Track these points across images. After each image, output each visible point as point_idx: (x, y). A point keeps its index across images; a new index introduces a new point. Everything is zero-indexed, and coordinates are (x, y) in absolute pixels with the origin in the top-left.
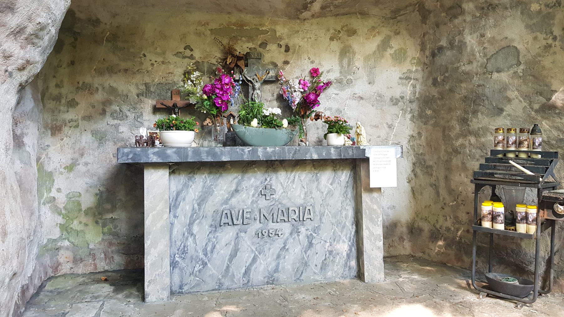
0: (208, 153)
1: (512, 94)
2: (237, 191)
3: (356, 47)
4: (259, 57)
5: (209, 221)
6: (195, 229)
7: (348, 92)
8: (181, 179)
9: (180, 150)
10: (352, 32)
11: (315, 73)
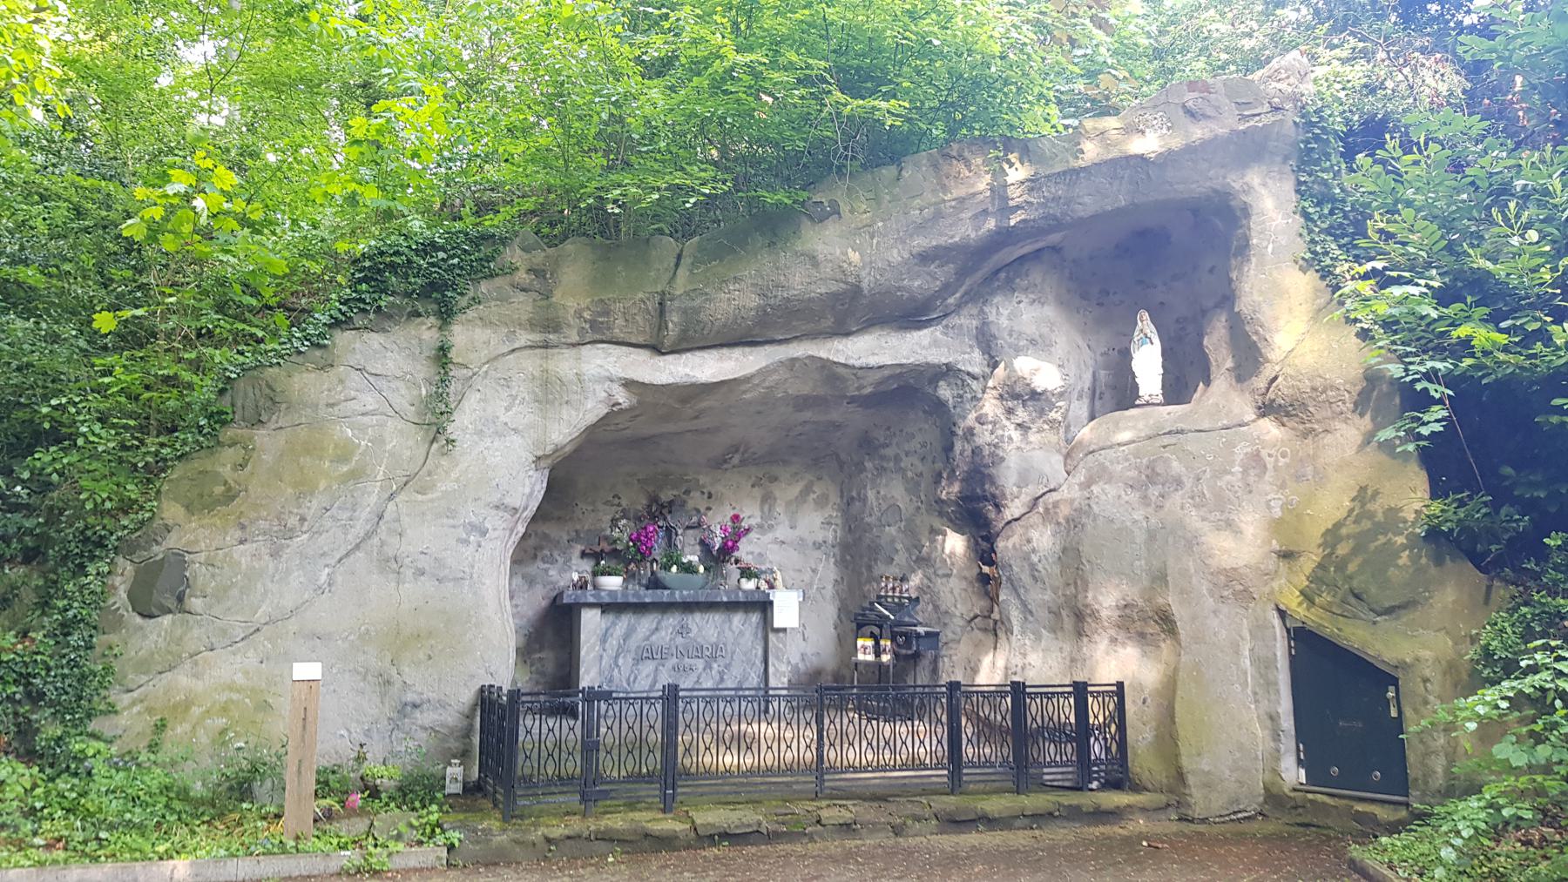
0: (634, 595)
1: (899, 546)
2: (657, 629)
3: (777, 493)
4: (683, 503)
5: (633, 655)
6: (621, 661)
7: (770, 536)
8: (611, 617)
9: (611, 593)
10: (774, 479)
11: (736, 518)
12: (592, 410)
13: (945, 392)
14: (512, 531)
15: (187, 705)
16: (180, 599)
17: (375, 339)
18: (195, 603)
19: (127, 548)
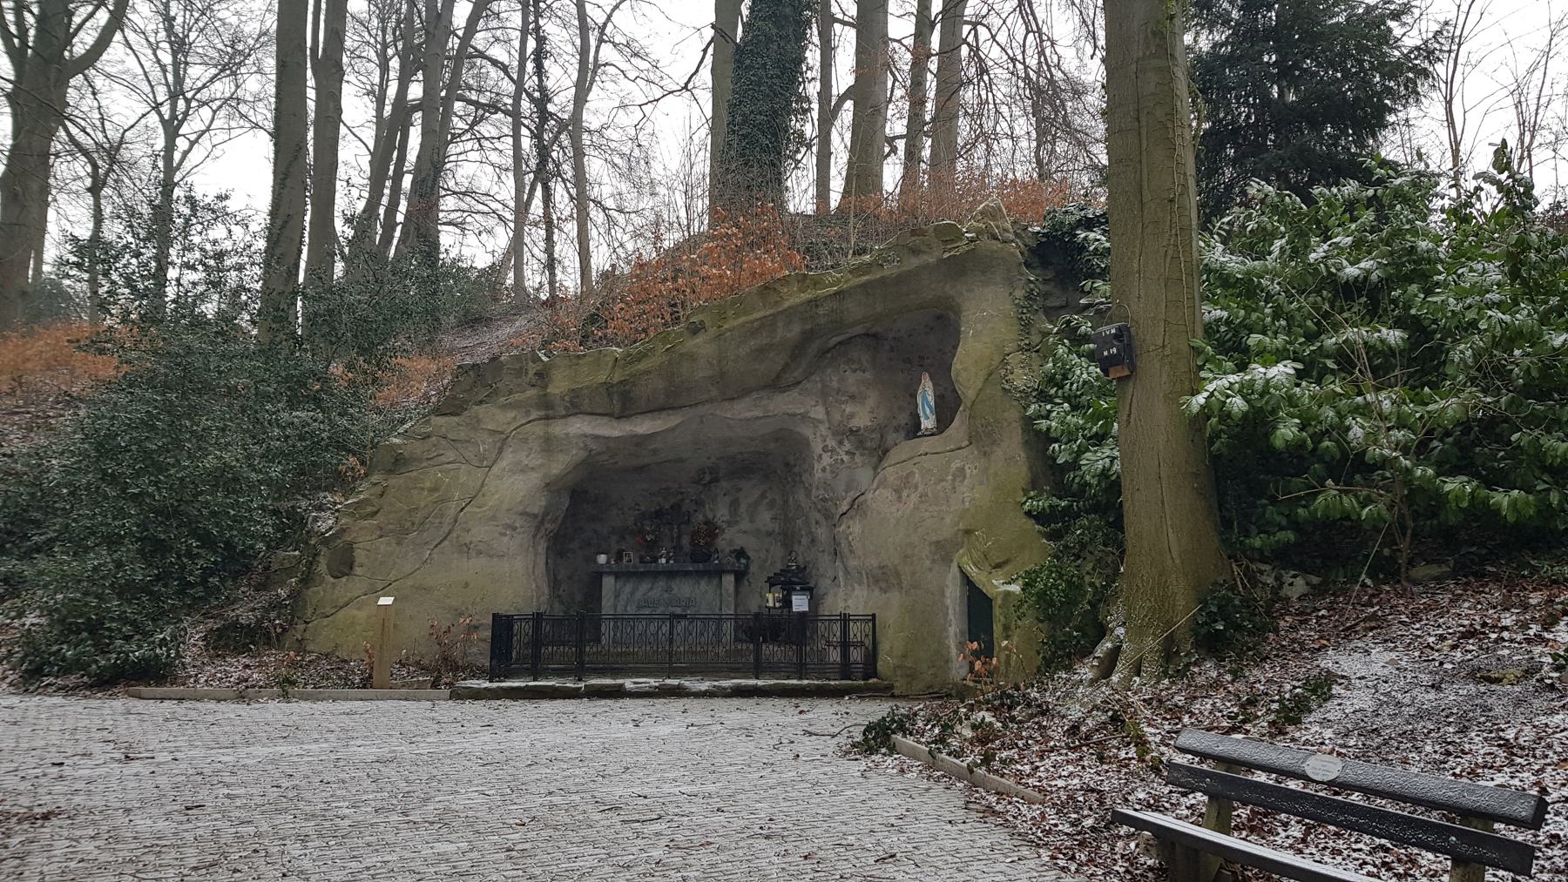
2: (652, 588)
7: (736, 528)
14: (538, 529)
16: (351, 568)
18: (358, 570)
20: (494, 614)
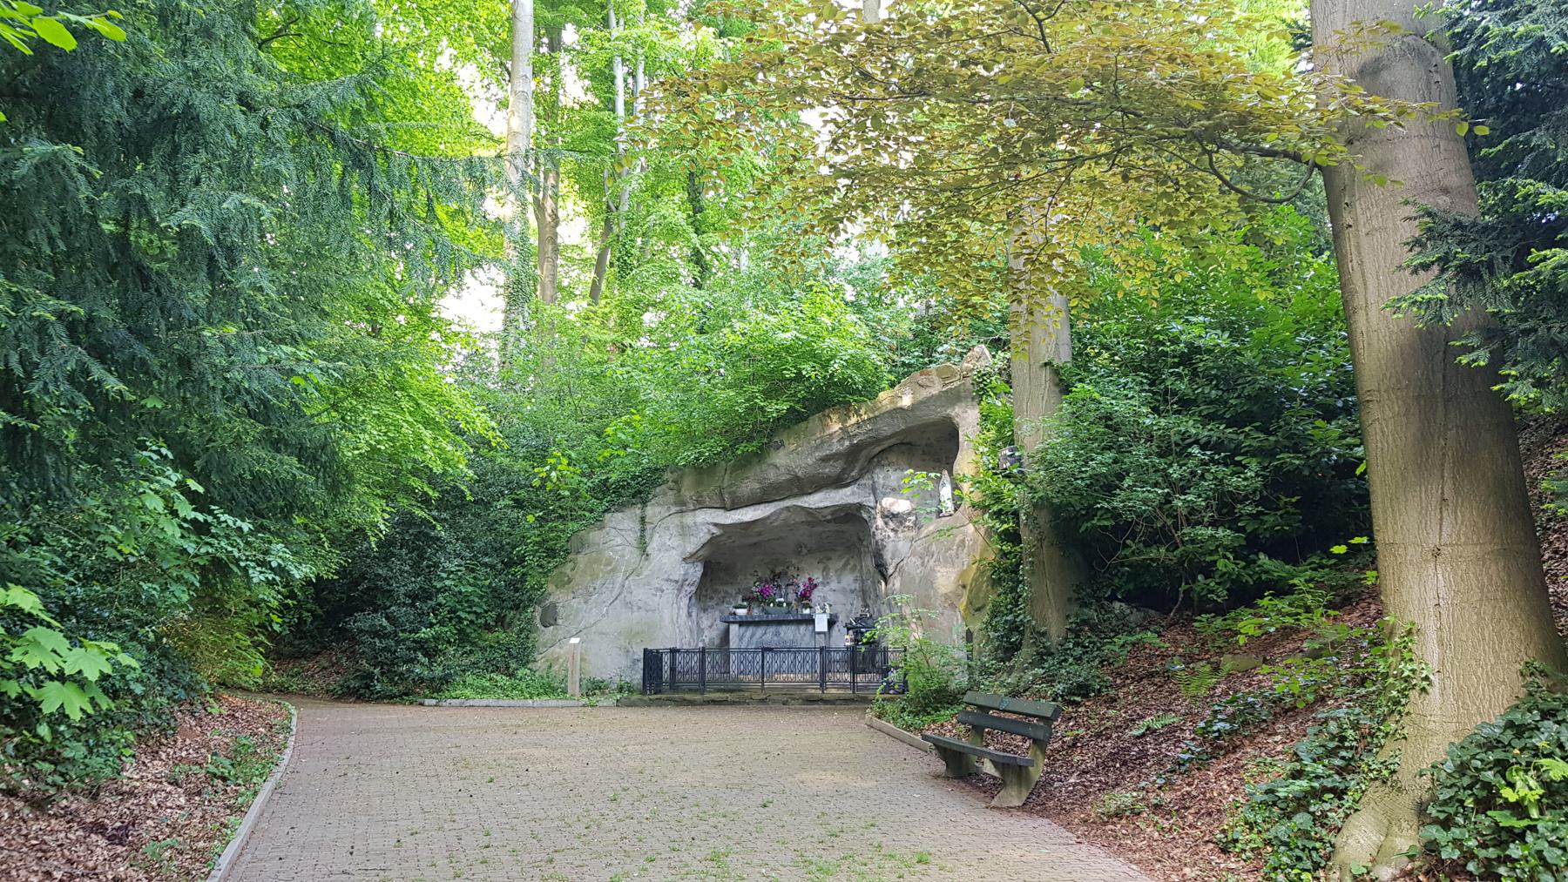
4: (786, 573)
7: (826, 589)
10: (830, 559)
12: (704, 537)
13: (865, 516)
14: (679, 590)
15: (558, 658)
17: (619, 515)
18: (560, 621)
19: (539, 603)
20: (645, 650)
